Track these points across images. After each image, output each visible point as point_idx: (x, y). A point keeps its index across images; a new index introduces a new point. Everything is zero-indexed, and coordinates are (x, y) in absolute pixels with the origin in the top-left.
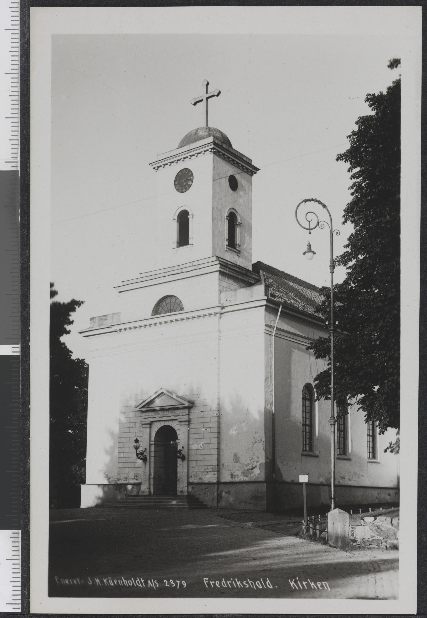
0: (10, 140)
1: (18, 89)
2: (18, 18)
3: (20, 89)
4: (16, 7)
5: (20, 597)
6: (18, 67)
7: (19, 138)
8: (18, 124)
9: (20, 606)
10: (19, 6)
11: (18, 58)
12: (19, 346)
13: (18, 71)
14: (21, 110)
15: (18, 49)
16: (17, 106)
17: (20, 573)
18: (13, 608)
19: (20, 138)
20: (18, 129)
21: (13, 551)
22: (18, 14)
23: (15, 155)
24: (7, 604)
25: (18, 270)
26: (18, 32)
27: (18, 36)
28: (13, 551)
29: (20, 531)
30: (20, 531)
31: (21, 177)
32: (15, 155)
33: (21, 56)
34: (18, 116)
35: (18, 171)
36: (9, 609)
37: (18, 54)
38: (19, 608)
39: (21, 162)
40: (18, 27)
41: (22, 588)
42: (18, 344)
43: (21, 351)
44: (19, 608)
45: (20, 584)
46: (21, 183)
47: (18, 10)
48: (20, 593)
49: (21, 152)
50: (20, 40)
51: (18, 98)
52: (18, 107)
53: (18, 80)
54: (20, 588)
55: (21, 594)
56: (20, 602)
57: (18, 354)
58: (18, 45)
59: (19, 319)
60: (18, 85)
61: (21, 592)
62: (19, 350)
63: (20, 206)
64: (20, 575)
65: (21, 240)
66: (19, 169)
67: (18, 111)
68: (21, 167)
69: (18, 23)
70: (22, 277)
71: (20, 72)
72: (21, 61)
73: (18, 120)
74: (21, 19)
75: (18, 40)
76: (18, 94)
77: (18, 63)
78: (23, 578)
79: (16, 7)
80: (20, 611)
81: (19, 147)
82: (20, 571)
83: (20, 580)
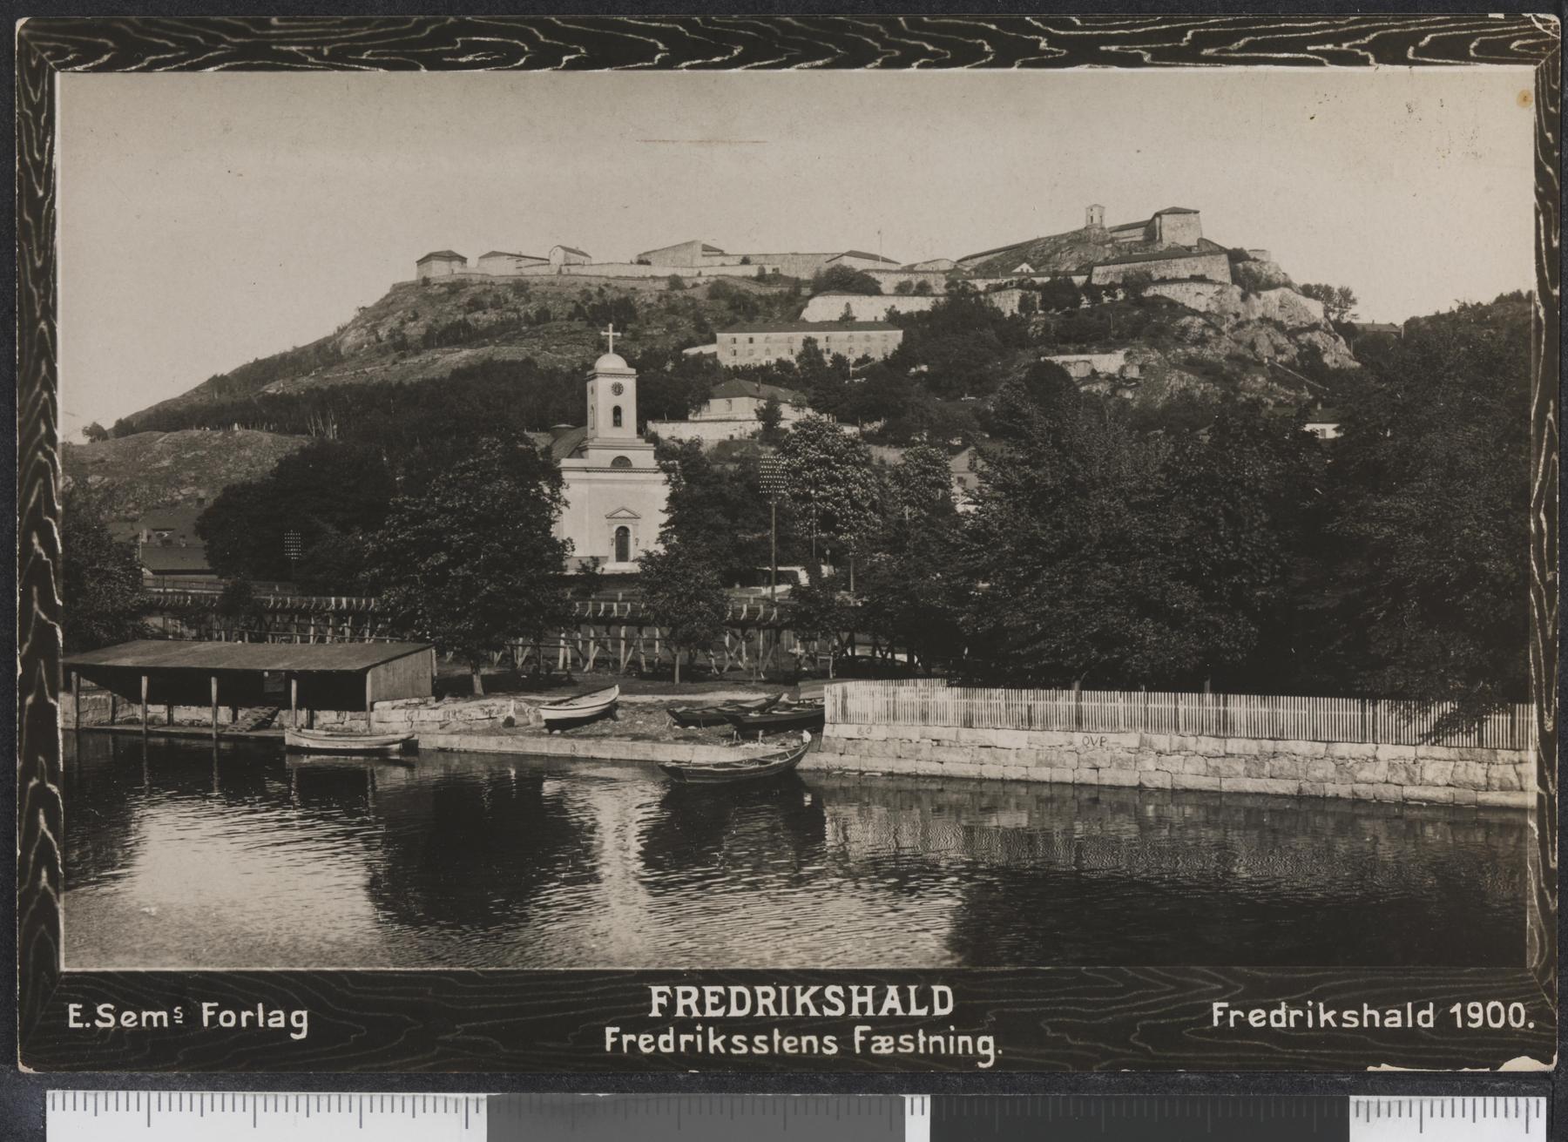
1: (292, 1096)
2: (122, 1094)
3: (291, 1090)
5: (1511, 1100)
6: (239, 1096)
7: (408, 1096)
8: (377, 1096)
9: (1532, 1100)
10: (93, 1092)
11: (218, 1096)
12: (908, 1098)
13: (249, 1096)
14: (343, 1091)
15: (197, 1096)
16: (332, 1098)
17: (1453, 1100)
19: (409, 1091)
20: (387, 1096)
21: (1400, 1115)
22: (112, 1095)
23: (451, 1106)
26: (154, 1095)
27: (165, 1095)
28: (1400, 1115)
29: (1353, 1099)
30: (1353, 1099)
31: (502, 1090)
32: (451, 1106)
34: (356, 1096)
35: (490, 1102)
36: (1540, 1125)
37: (207, 1095)
38: (1538, 1102)
39: (468, 1091)
40: (144, 1095)
41: (1489, 1095)
42: (903, 1101)
43: (920, 1093)
44: (1538, 1102)
45: (1479, 1100)
46: (516, 1091)
47: (101, 1094)
48: (1501, 1100)
50: (175, 1090)
51: (313, 1096)
52: (334, 1096)
53: (271, 1095)
54: (1490, 1100)
55: (1503, 1098)
56: (1522, 1100)
57: (928, 1099)
58: (186, 1095)
60: (281, 1096)
62: (918, 1099)
64: (1458, 1100)
66: (483, 1096)
67: (345, 1096)
68: (478, 1091)
69: (133, 1094)
71: (252, 1090)
72: (224, 1089)
73: (366, 1096)
74: (123, 1088)
75: (175, 1095)
76: (303, 1096)
77: (229, 1095)
78: (1464, 1093)
80: (1543, 1101)
81: (430, 1096)
82: (1448, 1100)
83: (1469, 1100)
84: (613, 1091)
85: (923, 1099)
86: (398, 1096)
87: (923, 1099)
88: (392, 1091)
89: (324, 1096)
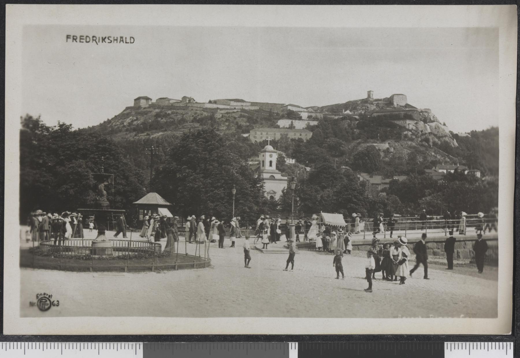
0: (117, 351)
1: (75, 343)
2: (15, 343)
3: (75, 341)
4: (6, 345)
5: (501, 343)
6: (56, 343)
7: (115, 343)
8: (104, 344)
9: (508, 343)
10: (5, 343)
11: (49, 343)
12: (290, 343)
13: (60, 344)
14: (93, 342)
15: (41, 343)
18: (510, 349)
19: (116, 342)
20: (108, 344)
22: (12, 343)
23: (130, 346)
24: (507, 354)
25: (227, 343)
26: (27, 343)
27: (30, 343)
29: (446, 343)
30: (446, 343)
31: (149, 342)
32: (130, 346)
33: (47, 341)
34: (97, 344)
36: (511, 352)
37: (45, 343)
38: (510, 344)
39: (136, 341)
40: (23, 343)
41: (494, 342)
42: (288, 344)
43: (294, 341)
44: (510, 344)
45: (490, 343)
46: (153, 341)
47: (8, 343)
48: (497, 343)
49: (128, 341)
50: (34, 341)
51: (82, 344)
52: (90, 344)
53: (67, 343)
54: (494, 343)
55: (498, 343)
56: (505, 343)
57: (297, 343)
58: (38, 343)
59: (267, 343)
60: (71, 343)
61: (496, 343)
62: (293, 343)
63: (173, 341)
64: (482, 343)
65: (201, 341)
66: (142, 343)
67: (93, 344)
68: (140, 342)
69: (19, 343)
70: (232, 341)
71: (61, 342)
73: (101, 344)
74: (16, 341)
75: (34, 343)
76: (78, 344)
77: (53, 343)
78: (485, 341)
79: (6, 345)
80: (512, 343)
81: (123, 343)
82: (479, 343)
83: (486, 343)
84: (187, 341)
85: (295, 344)
86: (112, 344)
87: (295, 344)
88: (110, 341)
89: (86, 343)
